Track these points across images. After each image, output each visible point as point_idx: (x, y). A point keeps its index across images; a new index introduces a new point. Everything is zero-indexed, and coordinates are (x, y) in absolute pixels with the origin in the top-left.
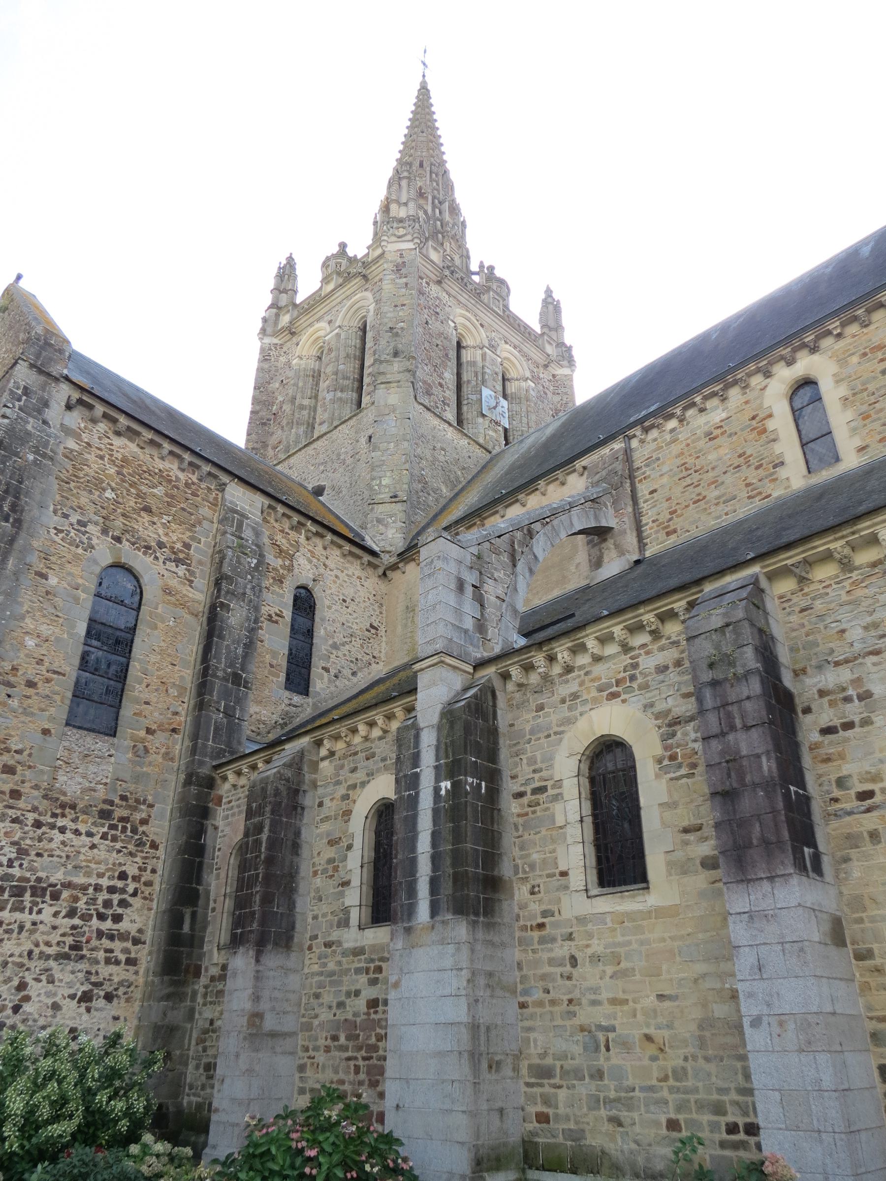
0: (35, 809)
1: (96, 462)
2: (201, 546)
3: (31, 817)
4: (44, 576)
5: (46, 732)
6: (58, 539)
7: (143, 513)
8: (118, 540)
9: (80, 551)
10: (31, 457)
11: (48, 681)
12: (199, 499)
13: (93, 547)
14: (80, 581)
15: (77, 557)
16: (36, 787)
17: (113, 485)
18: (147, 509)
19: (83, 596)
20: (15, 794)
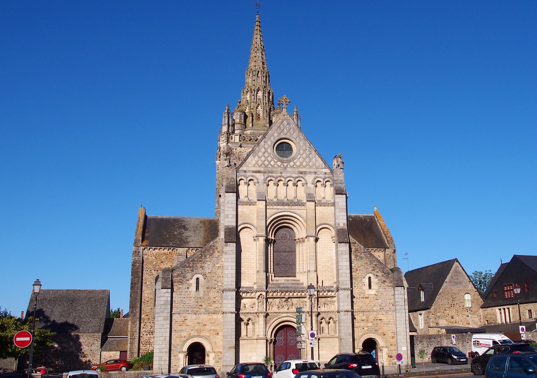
0: (152, 320)
1: (151, 258)
2: (175, 264)
3: (152, 322)
4: (146, 283)
5: (152, 308)
6: (147, 276)
7: (161, 263)
8: (158, 271)
9: (151, 276)
10: (138, 265)
11: (150, 300)
12: (173, 255)
13: (153, 274)
14: (152, 281)
15: (151, 277)
16: (152, 317)
17: (155, 260)
18: (162, 262)
19: (153, 284)
20: (149, 319)
